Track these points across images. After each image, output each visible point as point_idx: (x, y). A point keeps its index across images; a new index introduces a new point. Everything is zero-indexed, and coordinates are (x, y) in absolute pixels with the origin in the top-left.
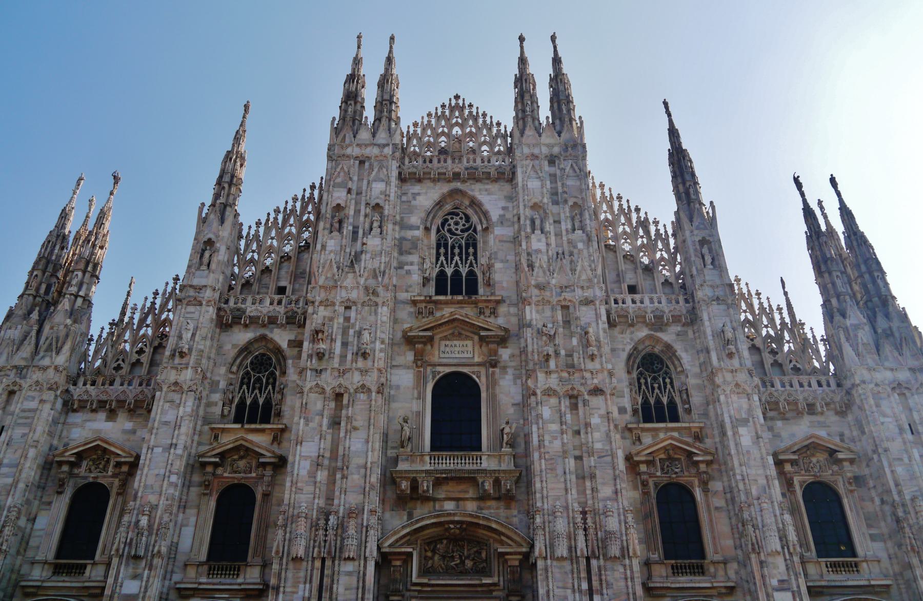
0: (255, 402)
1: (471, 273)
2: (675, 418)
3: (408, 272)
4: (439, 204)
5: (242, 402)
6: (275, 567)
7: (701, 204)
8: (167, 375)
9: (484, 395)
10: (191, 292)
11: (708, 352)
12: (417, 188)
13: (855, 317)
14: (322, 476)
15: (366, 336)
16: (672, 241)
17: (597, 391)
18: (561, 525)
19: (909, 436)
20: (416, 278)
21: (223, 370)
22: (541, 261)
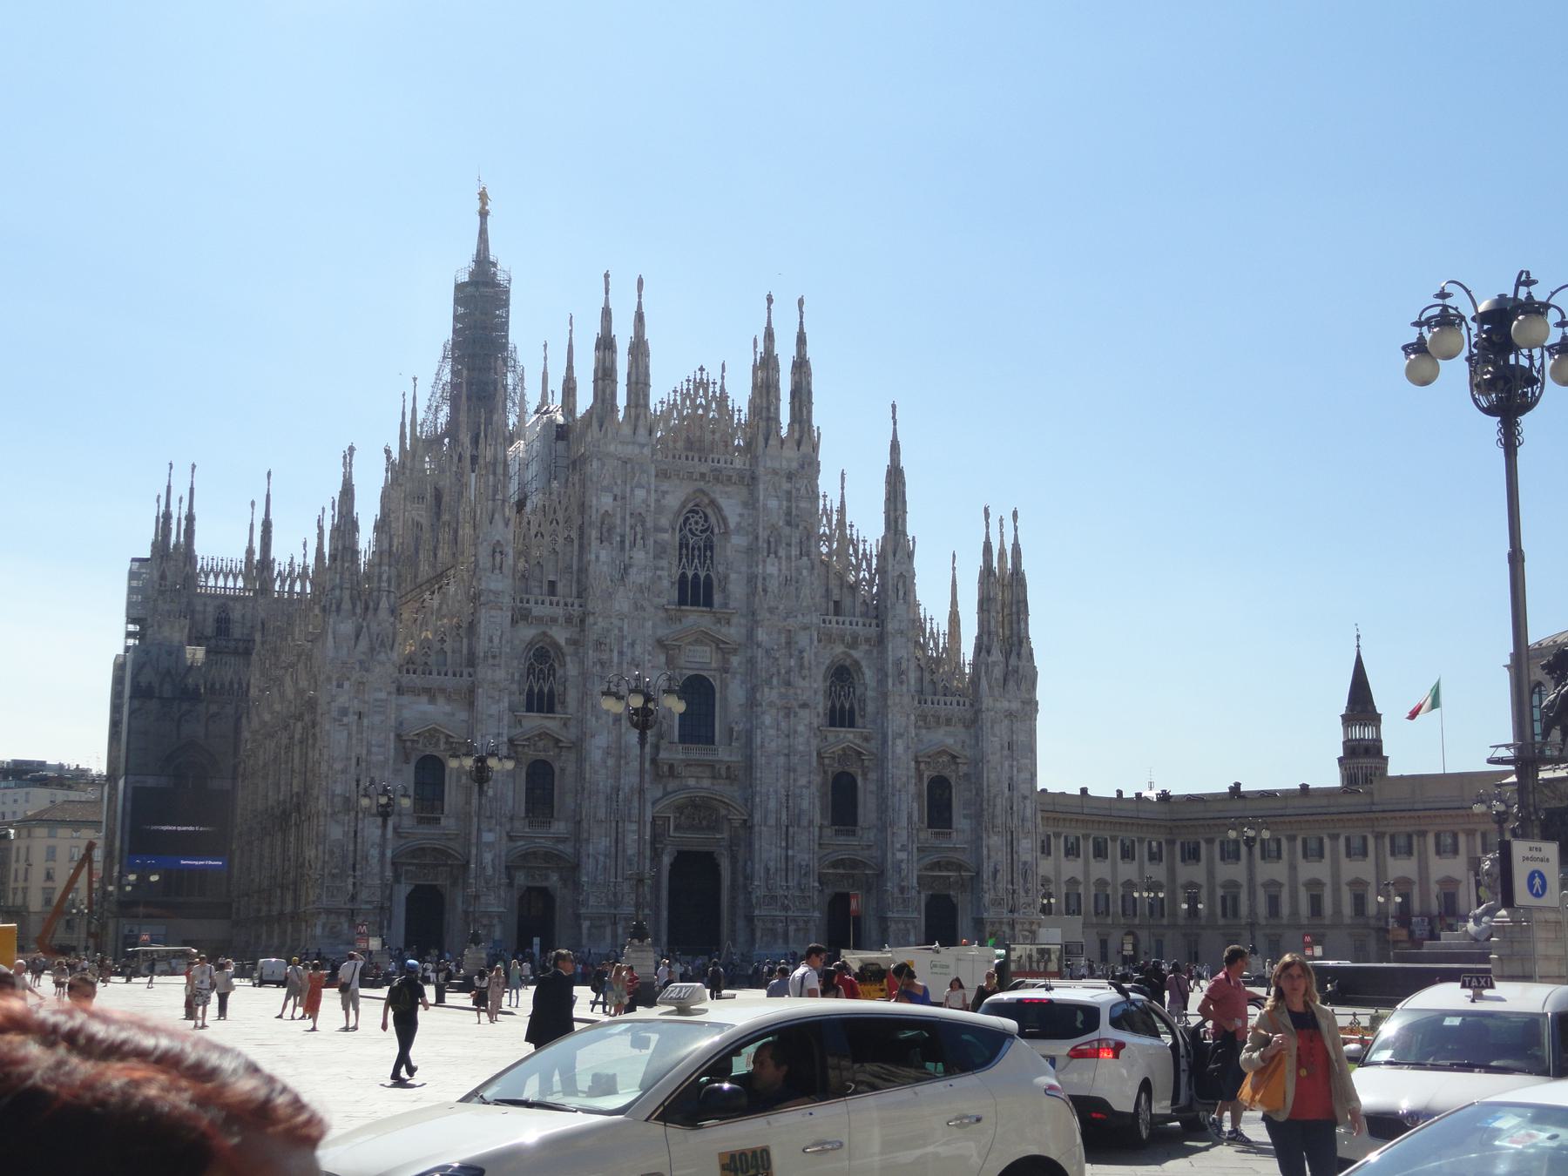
0: (541, 690)
1: (708, 577)
2: (852, 725)
3: (660, 577)
4: (683, 505)
5: (531, 689)
6: (585, 825)
7: (905, 534)
8: (484, 672)
9: (718, 695)
10: (492, 597)
11: (886, 676)
12: (665, 486)
13: (997, 656)
14: (611, 762)
15: (638, 649)
16: (874, 561)
17: (804, 706)
18: (772, 804)
19: (1006, 752)
20: (666, 583)
21: (515, 663)
22: (773, 585)
